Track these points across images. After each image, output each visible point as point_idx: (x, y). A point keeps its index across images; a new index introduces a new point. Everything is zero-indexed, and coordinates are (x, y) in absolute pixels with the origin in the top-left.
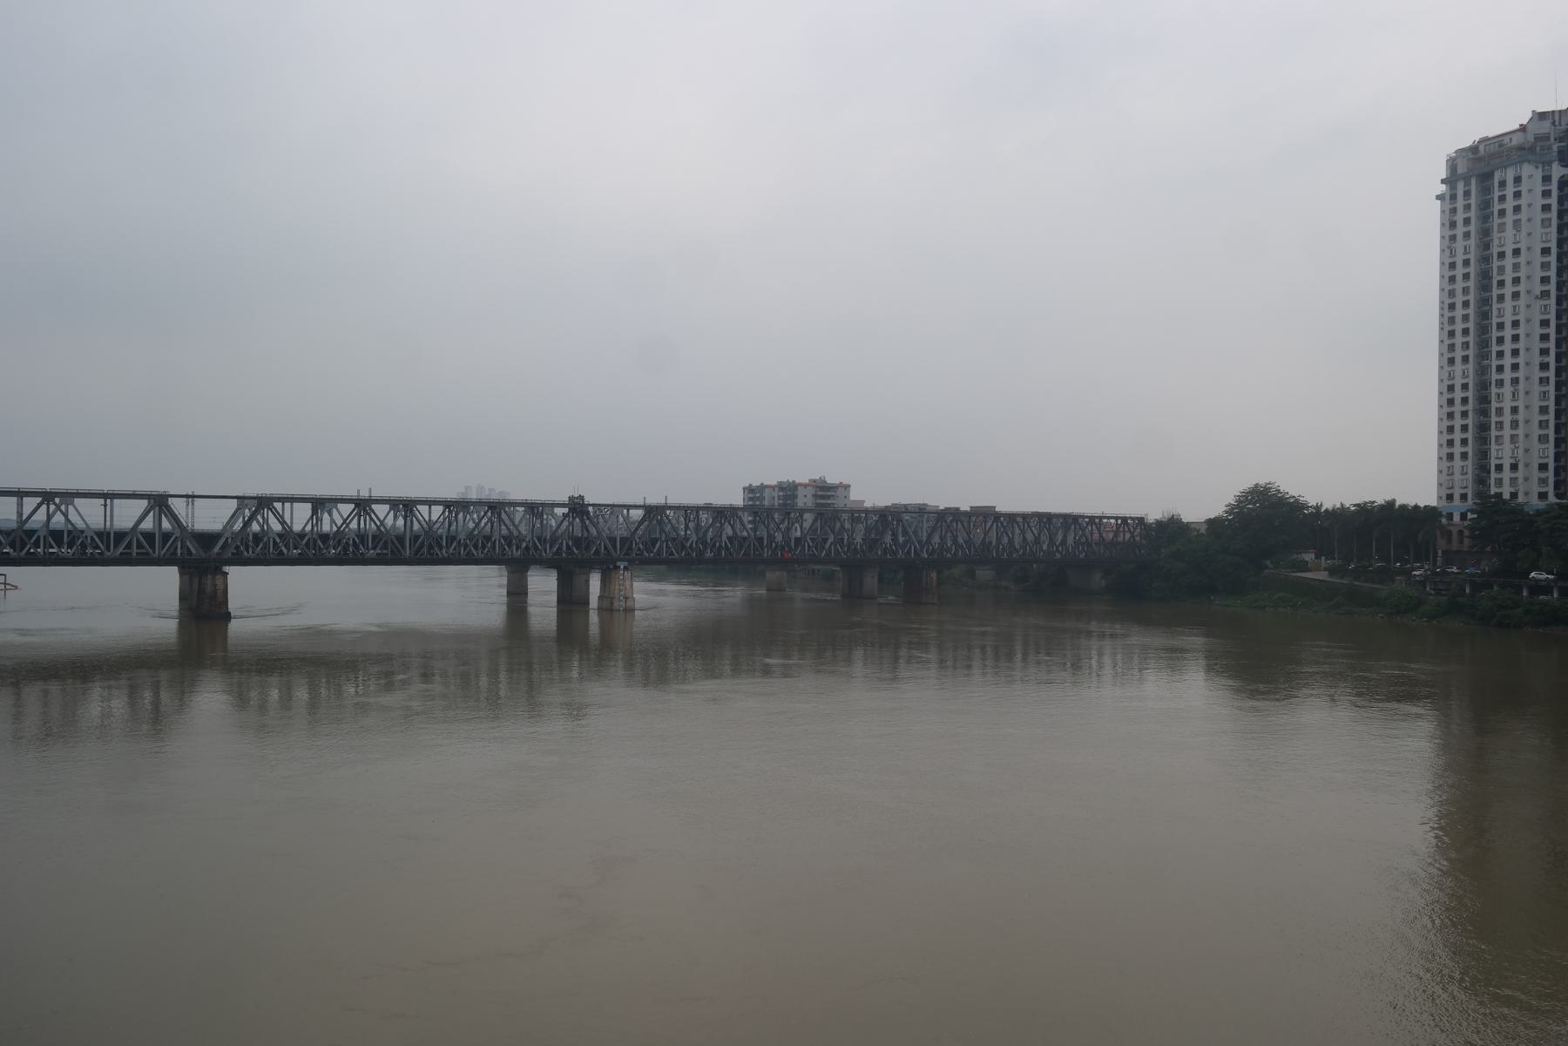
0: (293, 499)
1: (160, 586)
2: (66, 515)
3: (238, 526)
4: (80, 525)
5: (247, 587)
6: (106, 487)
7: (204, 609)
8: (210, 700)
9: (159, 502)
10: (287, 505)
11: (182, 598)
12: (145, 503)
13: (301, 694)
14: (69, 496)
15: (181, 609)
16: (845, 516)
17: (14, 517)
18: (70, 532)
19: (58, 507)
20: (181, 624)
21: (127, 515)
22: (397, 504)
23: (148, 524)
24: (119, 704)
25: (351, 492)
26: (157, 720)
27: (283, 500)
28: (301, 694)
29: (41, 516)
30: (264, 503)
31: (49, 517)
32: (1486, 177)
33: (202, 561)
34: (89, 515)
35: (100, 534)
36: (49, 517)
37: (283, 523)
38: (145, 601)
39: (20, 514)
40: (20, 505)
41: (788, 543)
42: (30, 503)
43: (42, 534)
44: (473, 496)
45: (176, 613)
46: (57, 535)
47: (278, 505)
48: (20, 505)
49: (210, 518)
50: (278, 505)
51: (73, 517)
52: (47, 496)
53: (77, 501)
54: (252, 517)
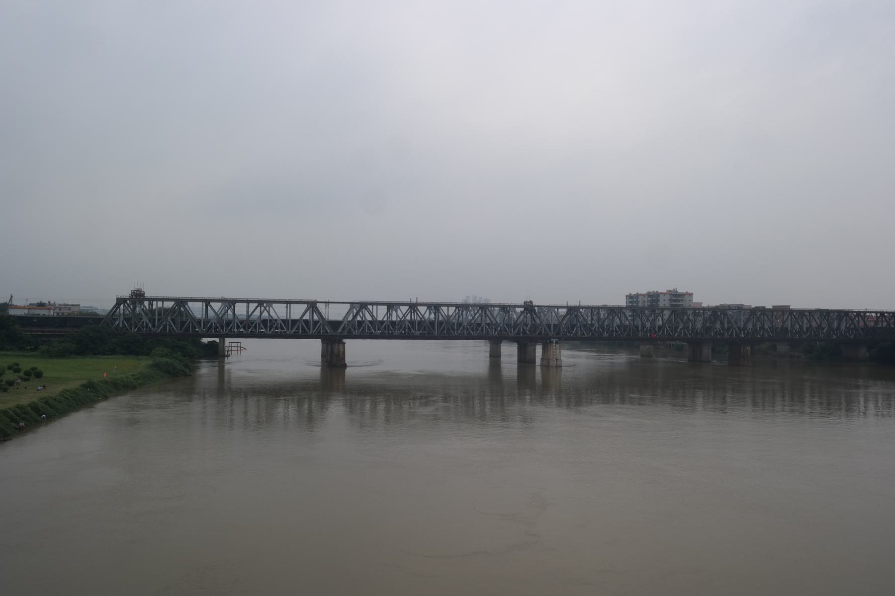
0: (378, 304)
1: (313, 348)
2: (269, 312)
3: (350, 318)
4: (275, 317)
5: (356, 351)
6: (287, 298)
7: (333, 361)
8: (336, 410)
9: (312, 306)
11: (323, 356)
12: (305, 306)
13: (381, 407)
14: (270, 302)
15: (323, 361)
16: (690, 312)
19: (265, 308)
20: (322, 369)
21: (297, 312)
22: (429, 306)
23: (307, 317)
26: (310, 419)
27: (372, 304)
28: (381, 407)
29: (257, 313)
30: (363, 306)
31: (261, 313)
33: (334, 336)
34: (279, 312)
35: (284, 321)
36: (261, 313)
37: (372, 316)
39: (248, 312)
40: (248, 307)
42: (253, 306)
43: (258, 322)
44: (471, 301)
45: (320, 364)
46: (264, 322)
47: (370, 307)
48: (248, 307)
49: (337, 313)
50: (370, 307)
52: (260, 303)
53: (274, 305)
54: (357, 313)
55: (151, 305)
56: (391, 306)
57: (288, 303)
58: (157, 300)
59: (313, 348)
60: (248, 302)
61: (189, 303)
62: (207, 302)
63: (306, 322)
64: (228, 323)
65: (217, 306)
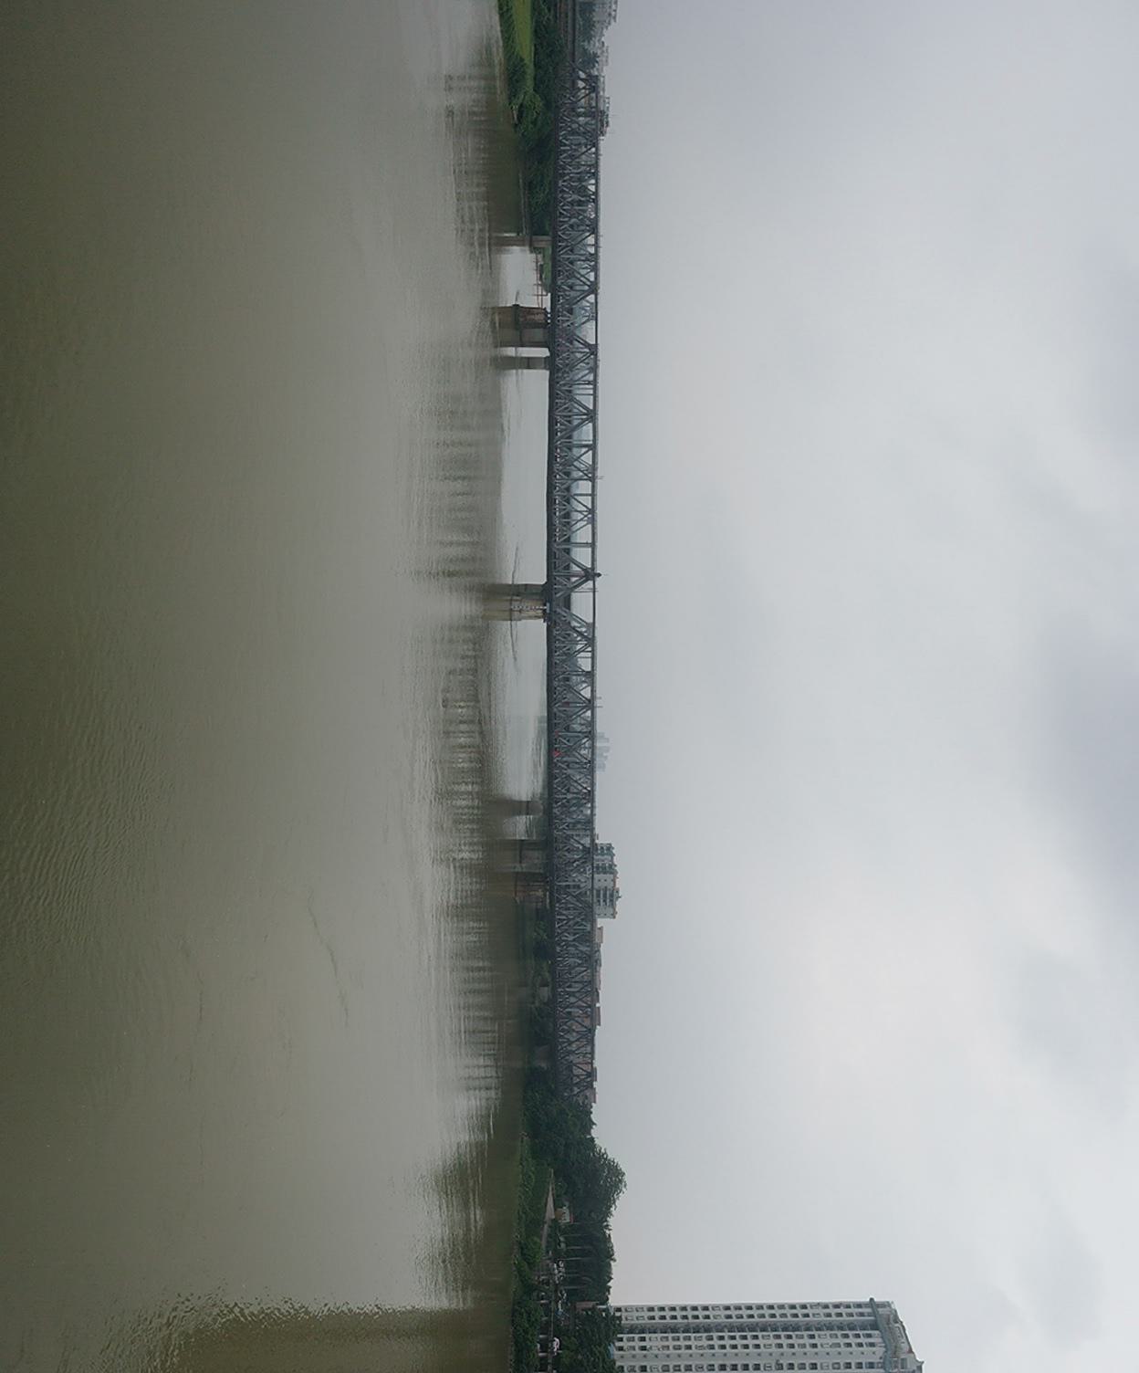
0: (593, 658)
1: (536, 573)
2: (582, 519)
3: (574, 624)
4: (574, 528)
6: (598, 544)
7: (514, 596)
8: (456, 607)
9: (590, 575)
10: (590, 654)
14: (593, 521)
15: (518, 585)
16: (589, 1049)
17: (578, 492)
18: (568, 523)
19: (586, 516)
20: (510, 585)
21: (582, 556)
22: (592, 723)
23: (575, 568)
24: (453, 552)
25: (598, 694)
27: (593, 652)
29: (581, 508)
30: (591, 641)
31: (580, 512)
32: (875, 1326)
34: (583, 534)
35: (568, 540)
36: (580, 512)
37: (579, 651)
38: (526, 562)
40: (587, 495)
41: (568, 1007)
42: (587, 501)
45: (515, 583)
46: (567, 515)
47: (589, 649)
48: (587, 495)
49: (581, 604)
51: (579, 525)
52: (592, 511)
53: (590, 526)
54: (580, 634)
55: (589, 383)
56: (590, 676)
57: (593, 545)
58: (595, 389)
59: (536, 573)
60: (593, 495)
61: (591, 425)
62: (593, 447)
63: (568, 567)
64: (568, 474)
65: (588, 458)
